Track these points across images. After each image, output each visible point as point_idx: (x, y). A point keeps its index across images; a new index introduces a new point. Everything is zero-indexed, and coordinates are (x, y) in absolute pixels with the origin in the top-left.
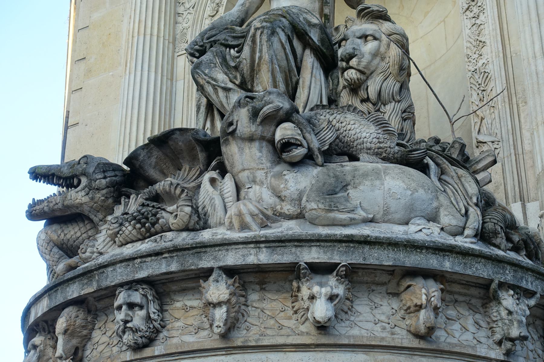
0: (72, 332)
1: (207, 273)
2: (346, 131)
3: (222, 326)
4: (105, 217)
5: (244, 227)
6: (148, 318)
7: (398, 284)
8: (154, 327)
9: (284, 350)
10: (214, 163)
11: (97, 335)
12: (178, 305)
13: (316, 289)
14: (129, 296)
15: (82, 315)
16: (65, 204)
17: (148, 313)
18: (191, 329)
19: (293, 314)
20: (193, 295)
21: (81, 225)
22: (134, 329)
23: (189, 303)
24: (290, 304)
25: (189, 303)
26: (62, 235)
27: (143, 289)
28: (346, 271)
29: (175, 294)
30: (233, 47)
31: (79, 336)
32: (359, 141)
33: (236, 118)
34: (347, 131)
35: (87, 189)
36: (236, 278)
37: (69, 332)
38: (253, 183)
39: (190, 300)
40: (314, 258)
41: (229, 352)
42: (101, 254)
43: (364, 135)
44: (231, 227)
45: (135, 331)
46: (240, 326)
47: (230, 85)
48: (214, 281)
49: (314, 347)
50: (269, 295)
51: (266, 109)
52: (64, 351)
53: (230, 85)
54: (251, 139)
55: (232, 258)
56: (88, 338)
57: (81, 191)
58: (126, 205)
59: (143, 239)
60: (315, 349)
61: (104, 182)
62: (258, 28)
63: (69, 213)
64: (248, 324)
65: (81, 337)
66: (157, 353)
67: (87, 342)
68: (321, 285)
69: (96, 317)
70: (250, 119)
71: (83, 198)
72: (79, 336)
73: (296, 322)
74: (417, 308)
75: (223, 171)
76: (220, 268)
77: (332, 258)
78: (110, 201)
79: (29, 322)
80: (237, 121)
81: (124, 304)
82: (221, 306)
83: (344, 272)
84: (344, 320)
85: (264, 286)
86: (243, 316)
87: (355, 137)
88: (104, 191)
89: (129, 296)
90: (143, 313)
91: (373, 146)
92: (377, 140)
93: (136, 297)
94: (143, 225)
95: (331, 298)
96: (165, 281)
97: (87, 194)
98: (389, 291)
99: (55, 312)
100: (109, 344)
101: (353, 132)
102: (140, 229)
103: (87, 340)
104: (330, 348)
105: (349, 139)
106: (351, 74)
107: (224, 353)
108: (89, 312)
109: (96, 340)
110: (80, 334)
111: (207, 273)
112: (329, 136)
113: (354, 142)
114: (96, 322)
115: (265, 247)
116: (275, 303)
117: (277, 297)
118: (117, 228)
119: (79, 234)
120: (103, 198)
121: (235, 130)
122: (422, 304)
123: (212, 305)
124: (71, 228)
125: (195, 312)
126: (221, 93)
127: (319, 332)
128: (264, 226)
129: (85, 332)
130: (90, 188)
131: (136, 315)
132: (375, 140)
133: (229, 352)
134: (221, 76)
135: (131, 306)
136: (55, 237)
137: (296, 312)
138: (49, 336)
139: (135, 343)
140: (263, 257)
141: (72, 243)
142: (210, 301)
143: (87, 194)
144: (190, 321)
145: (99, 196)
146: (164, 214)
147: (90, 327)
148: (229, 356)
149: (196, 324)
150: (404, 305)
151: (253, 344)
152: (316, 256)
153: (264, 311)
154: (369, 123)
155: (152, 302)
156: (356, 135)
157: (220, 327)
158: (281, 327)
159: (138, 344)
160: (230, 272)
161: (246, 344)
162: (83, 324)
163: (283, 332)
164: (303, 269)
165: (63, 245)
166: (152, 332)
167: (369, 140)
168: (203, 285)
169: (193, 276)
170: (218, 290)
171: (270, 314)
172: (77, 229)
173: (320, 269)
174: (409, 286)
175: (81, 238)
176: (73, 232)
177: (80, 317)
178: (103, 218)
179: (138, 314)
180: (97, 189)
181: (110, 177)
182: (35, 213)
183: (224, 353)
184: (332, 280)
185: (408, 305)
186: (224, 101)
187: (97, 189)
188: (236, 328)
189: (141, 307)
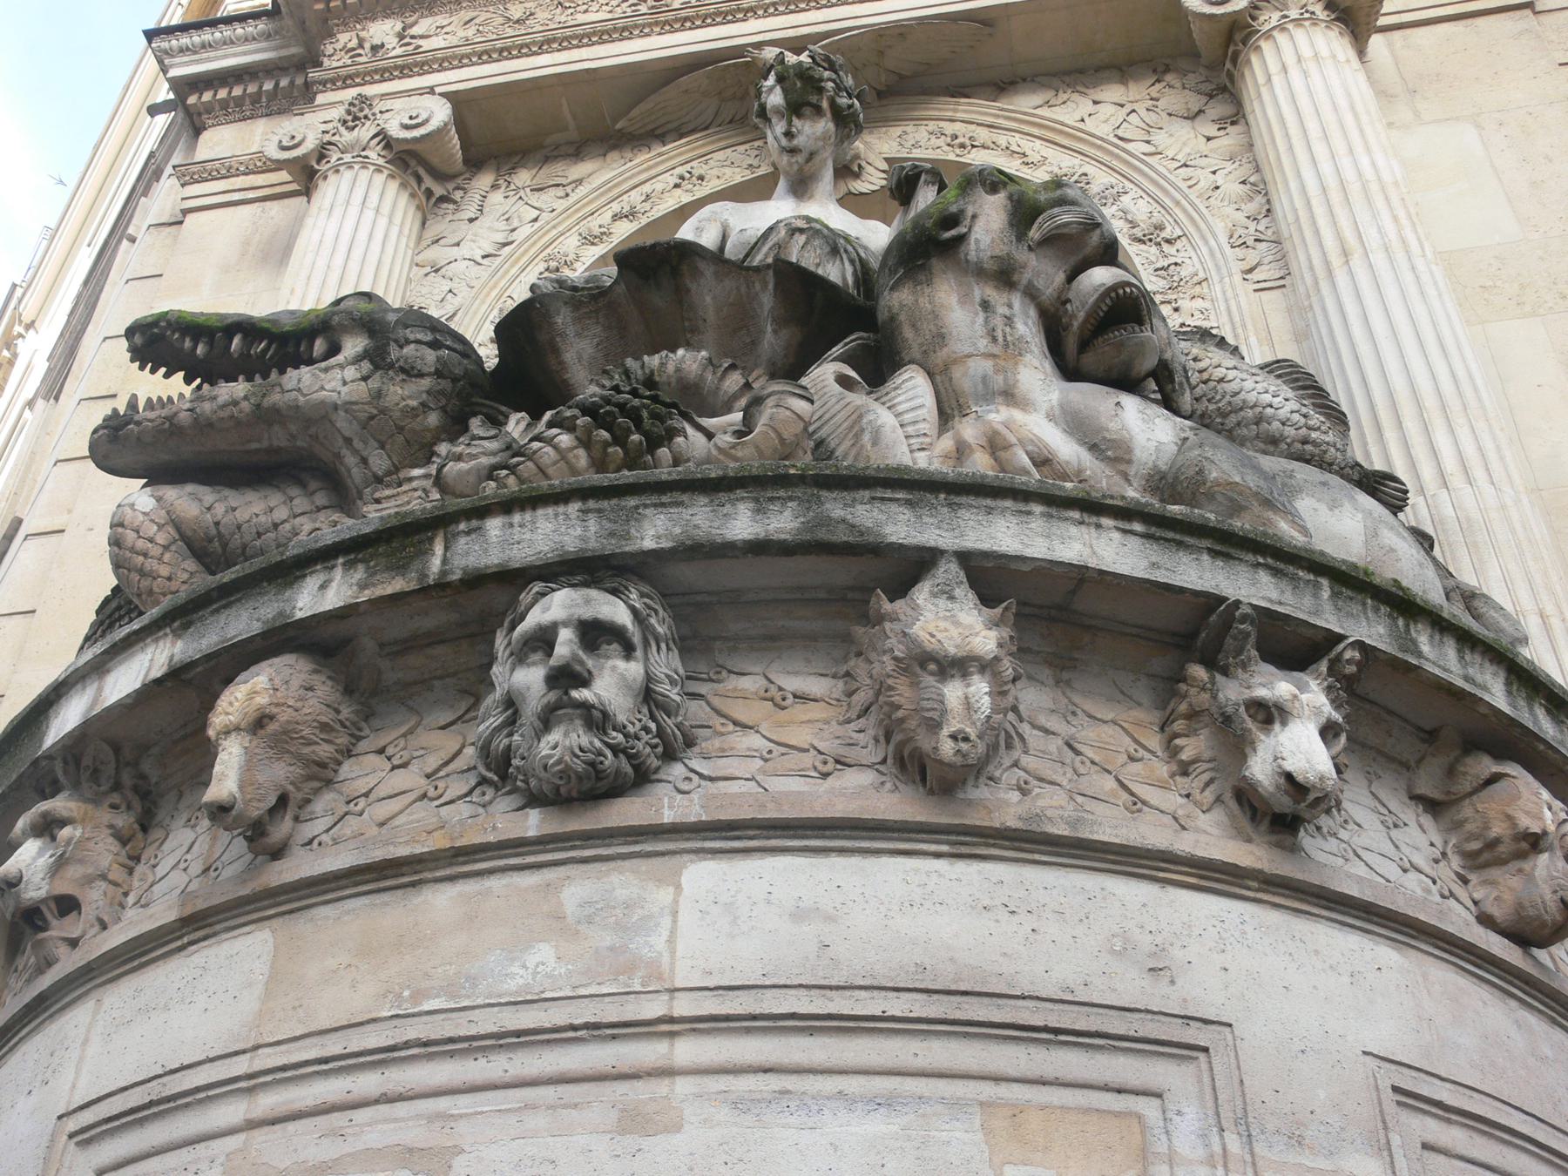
0: (285, 732)
2: (1205, 382)
3: (973, 737)
4: (397, 469)
6: (648, 695)
7: (1451, 772)
8: (661, 733)
9: (1161, 875)
11: (362, 773)
12: (749, 684)
14: (588, 601)
15: (325, 689)
16: (267, 402)
17: (649, 678)
18: (808, 759)
19: (1172, 775)
20: (808, 661)
21: (294, 491)
22: (595, 712)
23: (792, 683)
24: (1154, 741)
25: (792, 683)
26: (220, 509)
27: (642, 595)
28: (1358, 664)
29: (733, 650)
31: (299, 757)
32: (1250, 413)
33: (970, 211)
34: (1212, 384)
35: (366, 366)
36: (1006, 609)
37: (272, 727)
38: (1000, 399)
39: (796, 673)
40: (1270, 601)
41: (964, 850)
43: (1267, 398)
45: (597, 719)
46: (997, 774)
48: (934, 595)
49: (1255, 884)
50: (1089, 706)
52: (241, 788)
56: (322, 775)
57: (341, 367)
60: (1260, 895)
61: (430, 356)
62: (801, 231)
63: (265, 444)
64: (1022, 774)
65: (308, 762)
66: (668, 817)
67: (317, 791)
69: (368, 715)
70: (1011, 225)
71: (345, 390)
72: (299, 757)
73: (1184, 800)
74: (1524, 845)
75: (876, 367)
76: (966, 558)
77: (1316, 613)
78: (433, 419)
79: (41, 741)
80: (974, 217)
81: (565, 624)
82: (965, 675)
83: (1354, 669)
84: (1325, 830)
85: (1065, 675)
86: (1009, 747)
87: (1237, 400)
88: (426, 383)
89: (588, 601)
90: (634, 669)
91: (1289, 431)
92: (1303, 420)
93: (616, 611)
94: (620, 439)
96: (707, 599)
97: (365, 379)
98: (1419, 791)
99: (195, 685)
100: (424, 796)
101: (1234, 386)
102: (606, 444)
103: (316, 784)
104: (1301, 900)
105: (1212, 407)
107: (945, 848)
108: (349, 691)
109: (362, 785)
110: (306, 750)
113: (1225, 415)
114: (367, 731)
115: (1118, 529)
116: (1105, 728)
117: (1110, 716)
118: (494, 454)
119: (281, 513)
120: (414, 403)
121: (962, 238)
122: (1545, 833)
123: (932, 667)
124: (251, 495)
125: (816, 711)
127: (1274, 838)
129: (324, 751)
131: (607, 672)
132: (1296, 417)
133: (964, 850)
135: (594, 634)
137: (1184, 770)
138: (115, 798)
139: (592, 764)
141: (247, 538)
142: (930, 645)
143: (365, 379)
144: (801, 736)
145: (402, 394)
146: (690, 430)
147: (343, 740)
148: (961, 867)
149: (821, 746)
150: (1472, 837)
151: (1061, 830)
152: (1274, 595)
153: (1077, 746)
154: (1272, 377)
155: (663, 646)
156: (1241, 396)
157: (966, 739)
158: (1137, 804)
159: (598, 772)
160: (990, 578)
161: (1034, 827)
162: (324, 719)
164: (1244, 618)
165: (211, 541)
166: (654, 747)
167: (1283, 413)
168: (887, 606)
169: (822, 595)
171: (1097, 759)
172: (275, 498)
174: (1494, 779)
175: (287, 526)
177: (319, 693)
178: (389, 473)
179: (614, 668)
180: (402, 370)
181: (449, 348)
182: (120, 445)
183: (945, 848)
185: (1497, 829)
187: (402, 370)
188: (983, 780)
189: (628, 651)
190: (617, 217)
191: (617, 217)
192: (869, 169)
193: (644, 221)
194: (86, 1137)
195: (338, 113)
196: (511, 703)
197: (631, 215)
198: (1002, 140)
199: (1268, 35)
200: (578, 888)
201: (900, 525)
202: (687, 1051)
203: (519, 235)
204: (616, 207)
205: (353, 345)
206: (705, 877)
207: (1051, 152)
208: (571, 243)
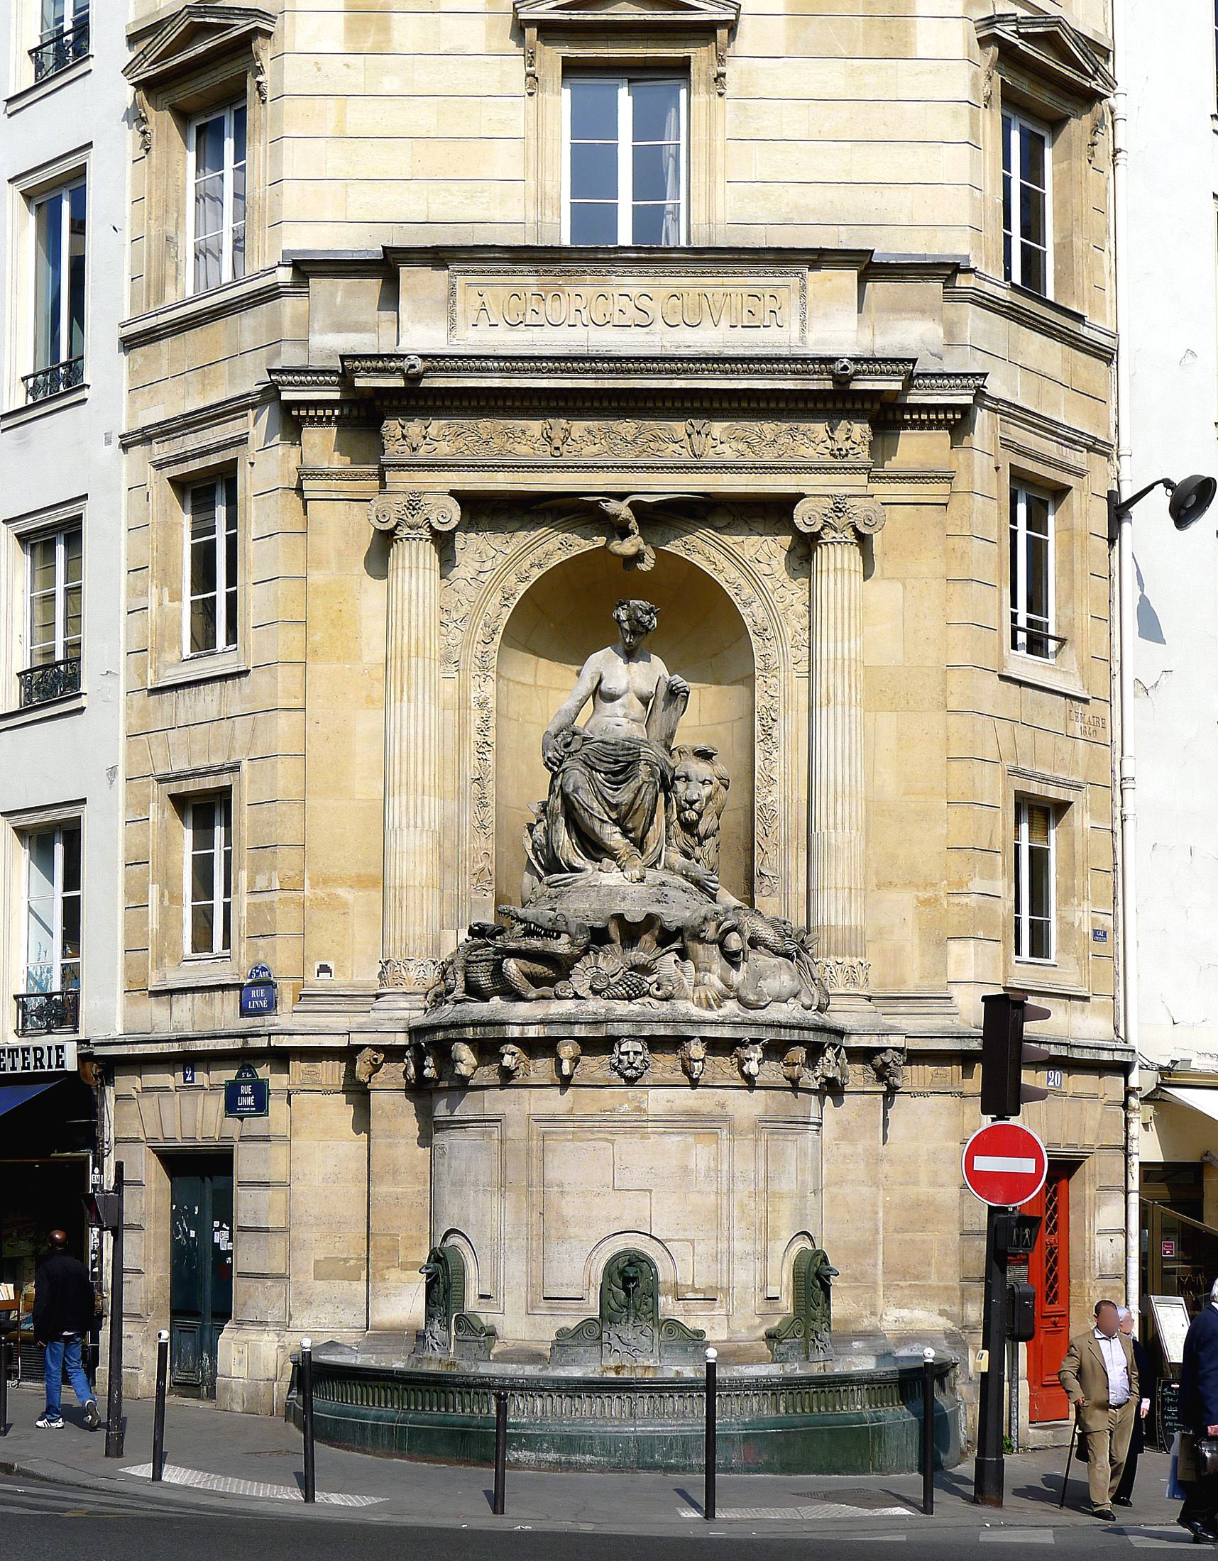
1: (690, 1038)
5: (710, 1007)
10: (673, 946)
13: (752, 1055)
30: (600, 772)
42: (577, 996)
44: (699, 1004)
45: (636, 1069)
47: (606, 818)
51: (726, 924)
53: (606, 818)
54: (712, 942)
55: (709, 1032)
58: (596, 959)
59: (630, 999)
68: (755, 1052)
95: (760, 1062)
106: (694, 816)
111: (690, 1038)
112: (747, 935)
126: (597, 824)
128: (719, 1007)
130: (572, 943)
134: (595, 804)
135: (636, 1053)
136: (526, 970)
140: (725, 1033)
160: (703, 1039)
163: (726, 1076)
170: (697, 1050)
173: (755, 1041)
176: (539, 969)
184: (758, 1047)
186: (597, 829)
190: (532, 566)
191: (532, 566)
192: (646, 556)
193: (545, 570)
194: (537, 1121)
195: (402, 499)
196: (620, 1061)
197: (540, 566)
198: (707, 549)
199: (826, 544)
200: (631, 1092)
201: (689, 1031)
202: (650, 1124)
203: (488, 565)
204: (531, 558)
205: (565, 938)
206: (652, 1092)
207: (726, 564)
208: (513, 578)
